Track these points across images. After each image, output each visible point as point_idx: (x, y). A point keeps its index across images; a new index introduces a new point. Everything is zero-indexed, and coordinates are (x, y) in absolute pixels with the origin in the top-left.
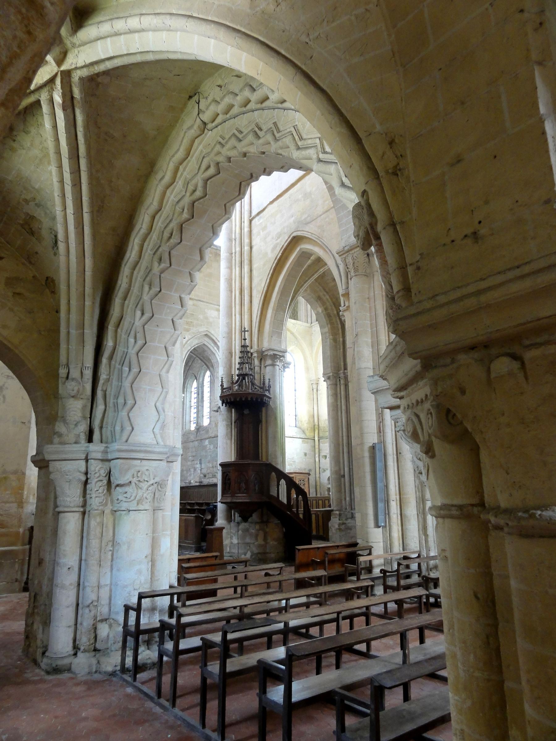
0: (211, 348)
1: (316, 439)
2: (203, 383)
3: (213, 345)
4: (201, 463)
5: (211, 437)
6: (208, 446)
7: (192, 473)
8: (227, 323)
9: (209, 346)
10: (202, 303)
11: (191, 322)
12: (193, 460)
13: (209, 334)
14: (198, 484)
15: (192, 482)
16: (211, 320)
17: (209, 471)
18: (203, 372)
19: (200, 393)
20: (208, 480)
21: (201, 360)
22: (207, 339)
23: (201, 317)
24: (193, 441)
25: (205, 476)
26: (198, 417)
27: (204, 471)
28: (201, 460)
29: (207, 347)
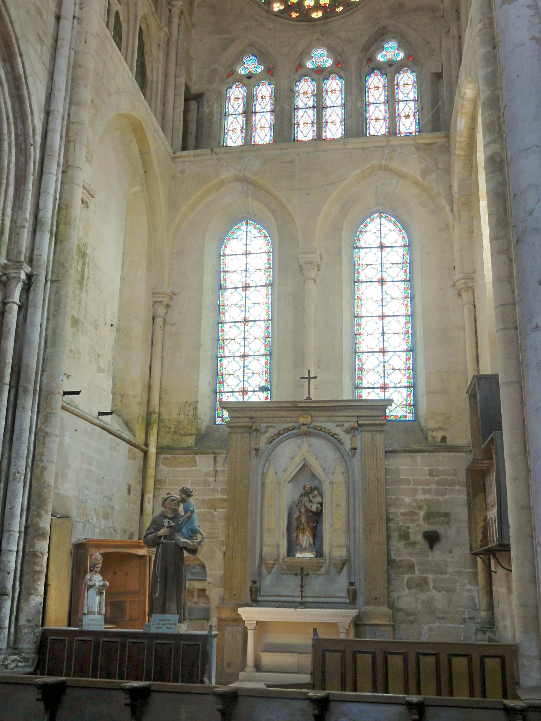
1: (152, 450)
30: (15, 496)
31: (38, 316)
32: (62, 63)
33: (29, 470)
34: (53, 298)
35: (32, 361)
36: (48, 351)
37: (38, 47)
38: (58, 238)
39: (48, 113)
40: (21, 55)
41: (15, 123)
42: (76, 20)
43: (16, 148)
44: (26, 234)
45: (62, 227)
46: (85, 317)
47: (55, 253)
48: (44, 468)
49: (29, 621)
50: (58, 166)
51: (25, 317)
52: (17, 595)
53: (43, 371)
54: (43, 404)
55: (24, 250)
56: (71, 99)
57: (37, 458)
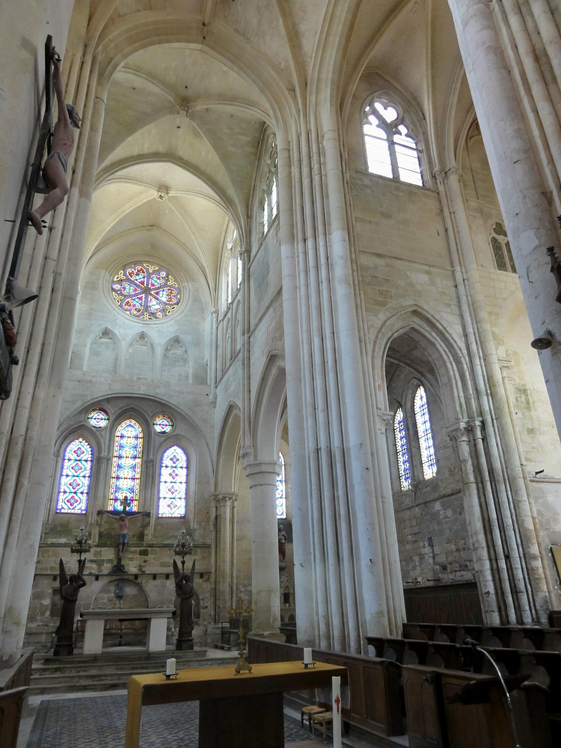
0: (427, 334)
2: (413, 411)
3: (428, 328)
4: (431, 545)
5: (445, 496)
6: (441, 513)
7: (418, 564)
8: (518, 130)
9: (422, 331)
10: (399, 262)
11: (387, 292)
12: (416, 541)
13: (419, 310)
14: (431, 584)
15: (420, 579)
16: (419, 287)
17: (450, 559)
18: (410, 391)
19: (410, 427)
20: (451, 576)
21: (409, 365)
22: (417, 320)
23: (402, 283)
24: (410, 508)
25: (444, 568)
26: (412, 467)
27: (442, 559)
28: (430, 539)
29: (419, 332)
30: (510, 538)
31: (493, 442)
32: (465, 307)
33: (515, 523)
34: (499, 427)
35: (497, 465)
36: (506, 456)
37: (448, 310)
38: (493, 395)
39: (466, 336)
40: (438, 321)
41: (450, 351)
42: (466, 281)
43: (455, 362)
44: (473, 402)
45: (492, 388)
46: (540, 425)
47: (493, 403)
48: (523, 520)
49: (541, 607)
50: (480, 358)
51: (487, 443)
52: (530, 592)
53: (507, 468)
54: (512, 485)
55: (475, 409)
56: (476, 321)
57: (518, 516)
